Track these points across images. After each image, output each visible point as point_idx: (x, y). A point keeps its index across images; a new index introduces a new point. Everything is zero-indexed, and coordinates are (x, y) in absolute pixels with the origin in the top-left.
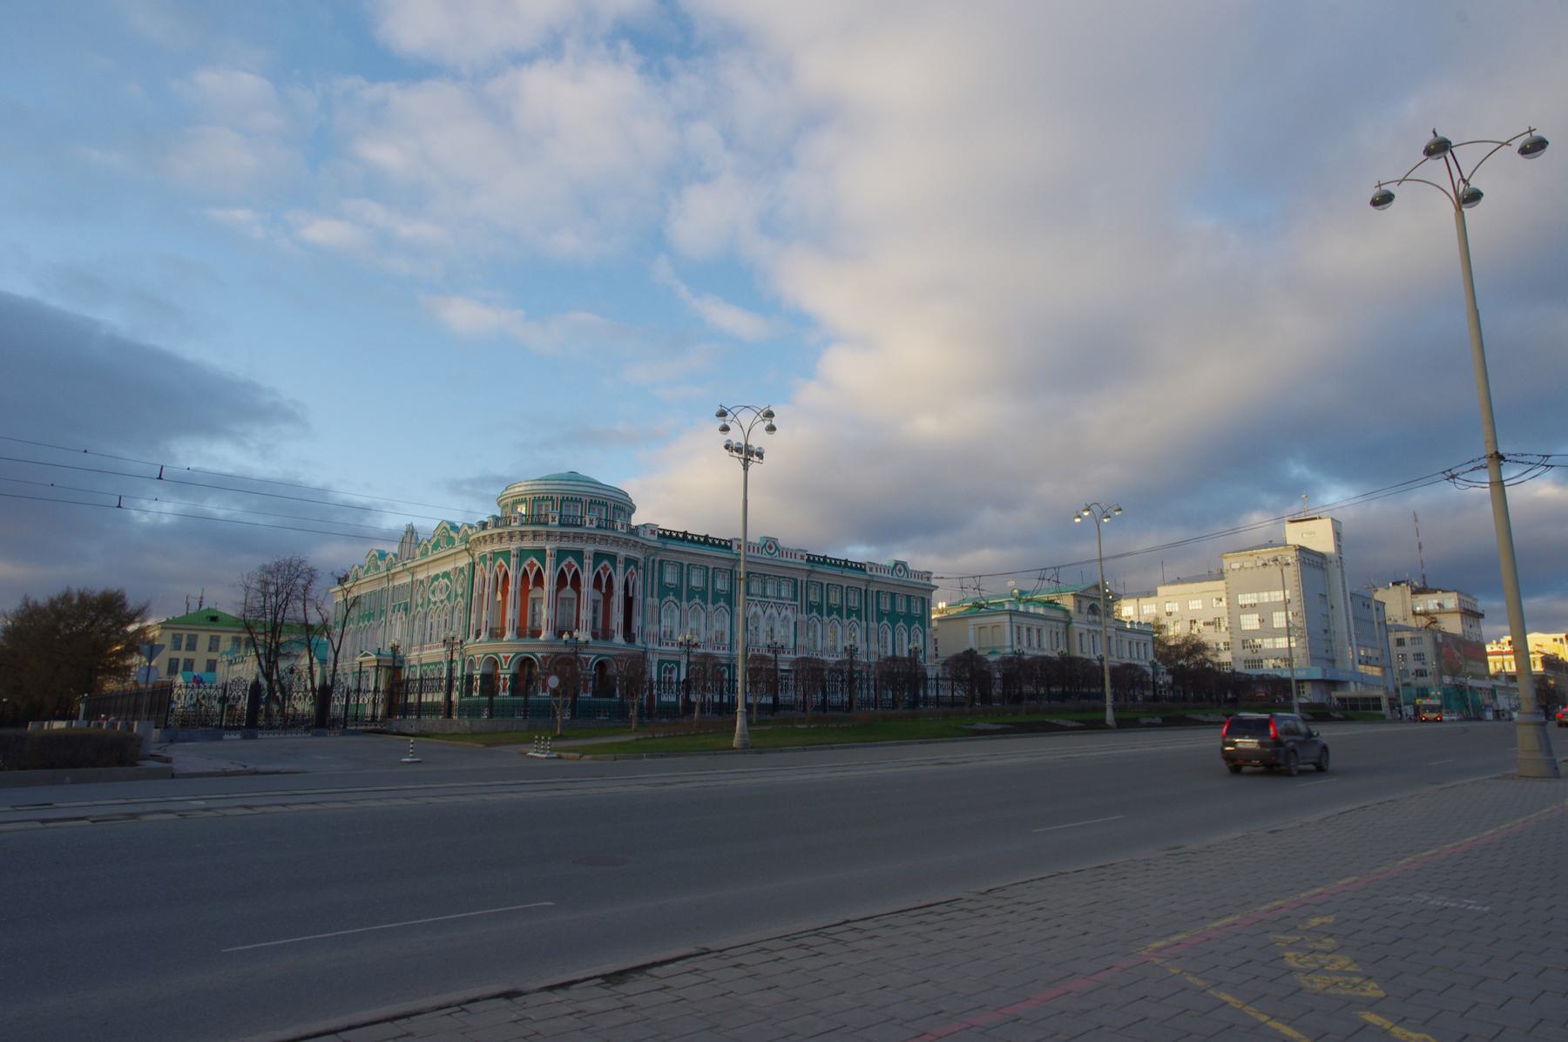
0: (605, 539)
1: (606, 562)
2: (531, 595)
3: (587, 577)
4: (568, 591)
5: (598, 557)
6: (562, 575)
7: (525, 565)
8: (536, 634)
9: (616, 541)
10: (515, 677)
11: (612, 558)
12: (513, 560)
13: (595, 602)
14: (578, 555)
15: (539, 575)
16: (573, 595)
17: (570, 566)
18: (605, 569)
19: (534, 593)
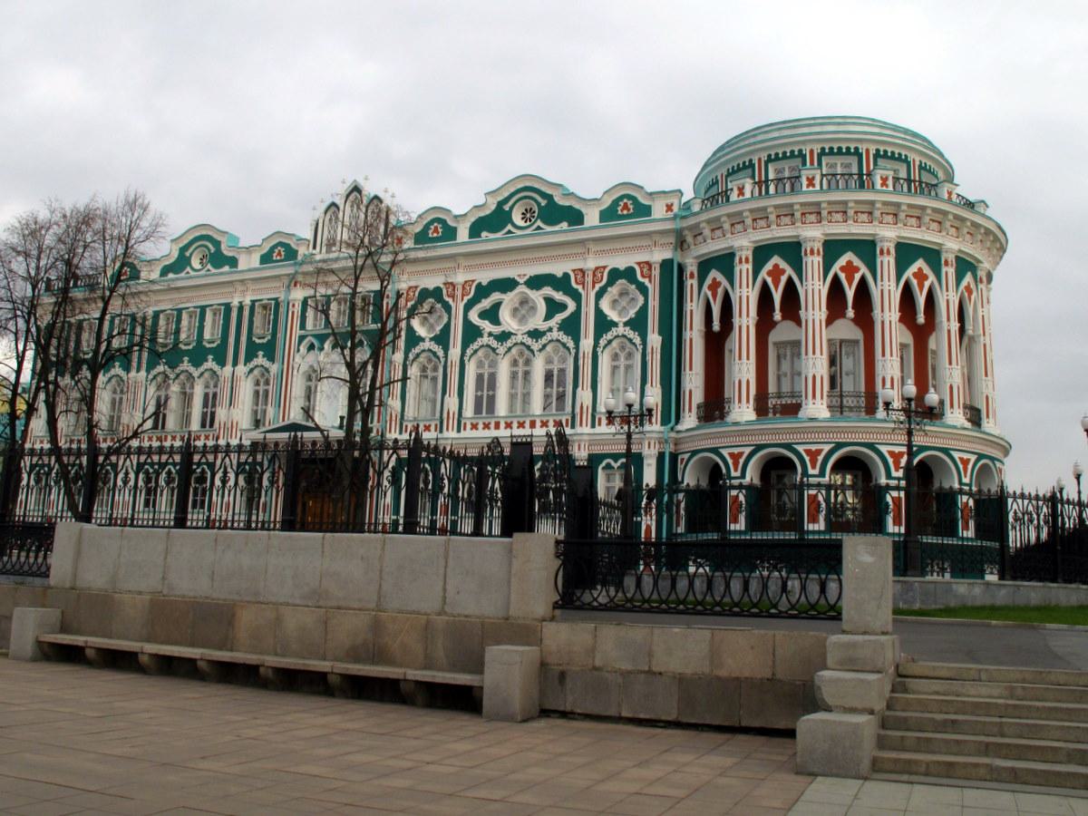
0: (918, 215)
1: (920, 264)
2: (774, 336)
3: (887, 293)
4: (847, 329)
5: (906, 253)
6: (836, 290)
7: (763, 274)
8: (793, 409)
9: (940, 219)
10: (758, 495)
11: (932, 256)
12: (743, 269)
13: (903, 346)
14: (866, 249)
15: (791, 294)
16: (857, 334)
17: (850, 269)
18: (920, 276)
19: (783, 331)
